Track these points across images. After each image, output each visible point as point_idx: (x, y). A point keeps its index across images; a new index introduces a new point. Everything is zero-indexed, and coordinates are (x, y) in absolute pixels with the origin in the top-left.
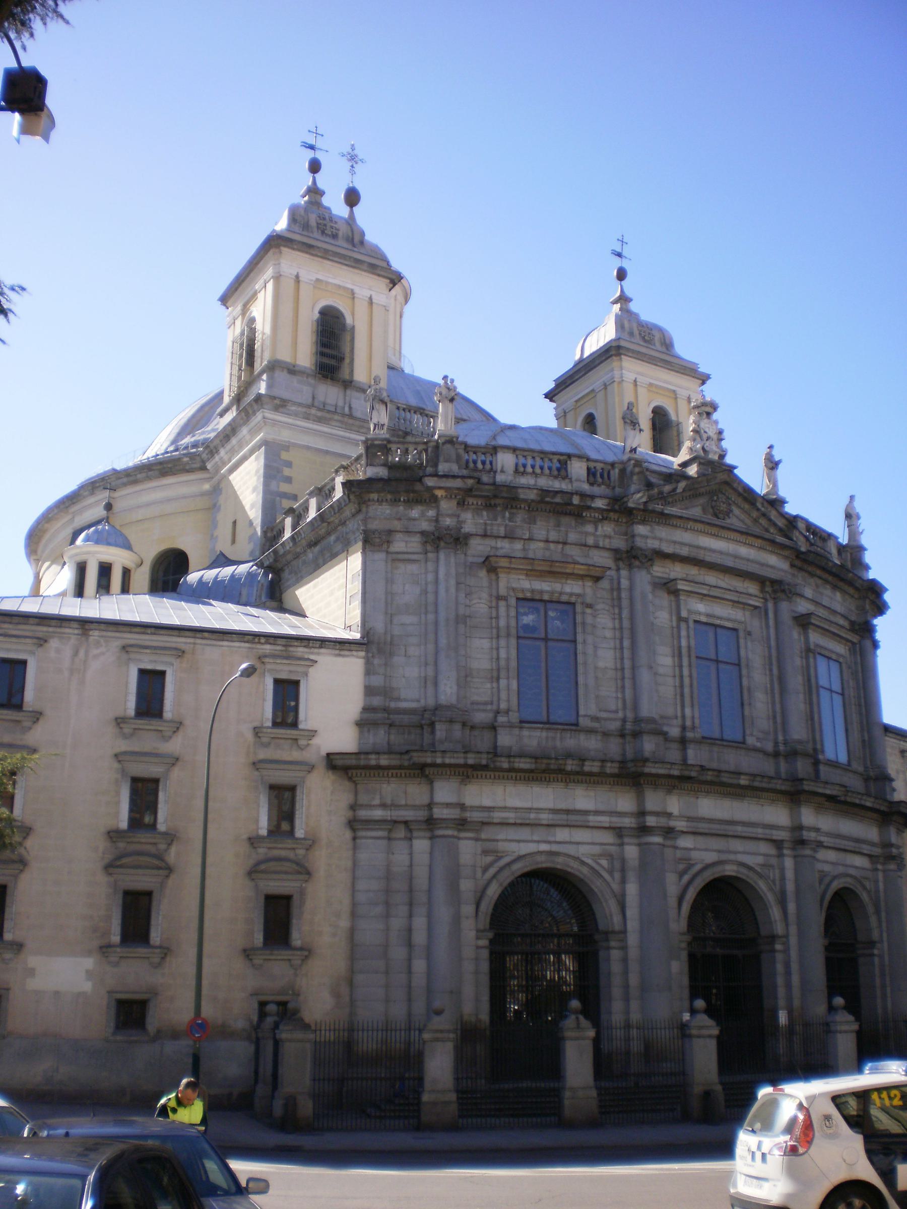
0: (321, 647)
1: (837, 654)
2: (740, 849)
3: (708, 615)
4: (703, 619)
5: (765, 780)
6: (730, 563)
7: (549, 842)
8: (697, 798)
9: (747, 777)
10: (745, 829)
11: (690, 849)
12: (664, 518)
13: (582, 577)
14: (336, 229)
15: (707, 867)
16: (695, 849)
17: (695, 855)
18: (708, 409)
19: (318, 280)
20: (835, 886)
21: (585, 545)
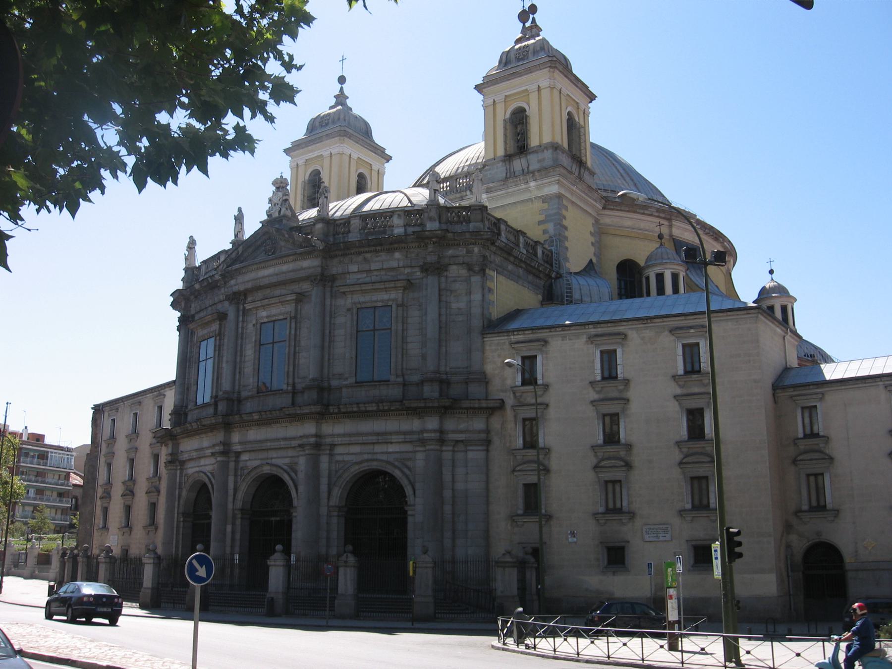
0: (165, 388)
1: (382, 301)
2: (275, 456)
3: (267, 317)
4: (265, 320)
5: (268, 413)
6: (274, 280)
7: (198, 467)
8: (247, 430)
9: (256, 414)
10: (273, 444)
11: (246, 461)
12: (239, 272)
13: (214, 320)
14: (329, 120)
15: (255, 468)
16: (250, 460)
17: (249, 463)
18: (278, 185)
19: (306, 160)
20: (355, 469)
21: (221, 301)
